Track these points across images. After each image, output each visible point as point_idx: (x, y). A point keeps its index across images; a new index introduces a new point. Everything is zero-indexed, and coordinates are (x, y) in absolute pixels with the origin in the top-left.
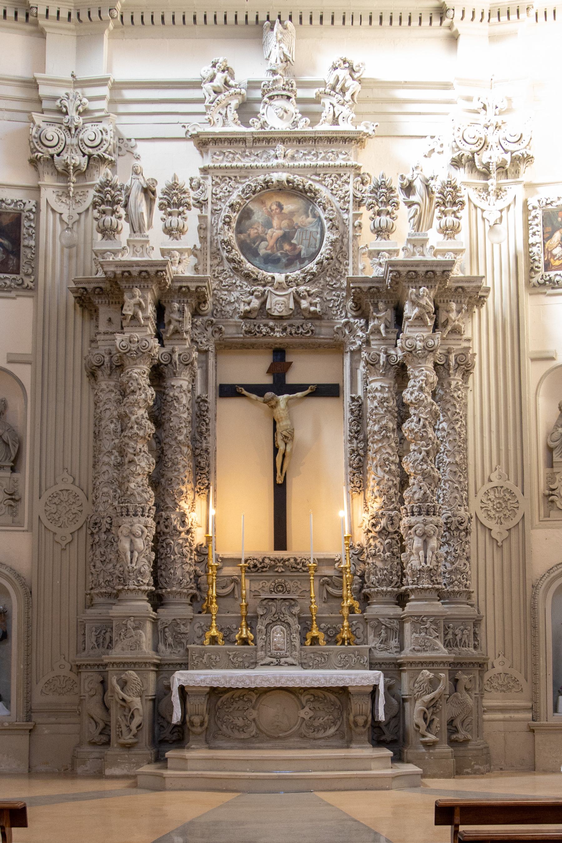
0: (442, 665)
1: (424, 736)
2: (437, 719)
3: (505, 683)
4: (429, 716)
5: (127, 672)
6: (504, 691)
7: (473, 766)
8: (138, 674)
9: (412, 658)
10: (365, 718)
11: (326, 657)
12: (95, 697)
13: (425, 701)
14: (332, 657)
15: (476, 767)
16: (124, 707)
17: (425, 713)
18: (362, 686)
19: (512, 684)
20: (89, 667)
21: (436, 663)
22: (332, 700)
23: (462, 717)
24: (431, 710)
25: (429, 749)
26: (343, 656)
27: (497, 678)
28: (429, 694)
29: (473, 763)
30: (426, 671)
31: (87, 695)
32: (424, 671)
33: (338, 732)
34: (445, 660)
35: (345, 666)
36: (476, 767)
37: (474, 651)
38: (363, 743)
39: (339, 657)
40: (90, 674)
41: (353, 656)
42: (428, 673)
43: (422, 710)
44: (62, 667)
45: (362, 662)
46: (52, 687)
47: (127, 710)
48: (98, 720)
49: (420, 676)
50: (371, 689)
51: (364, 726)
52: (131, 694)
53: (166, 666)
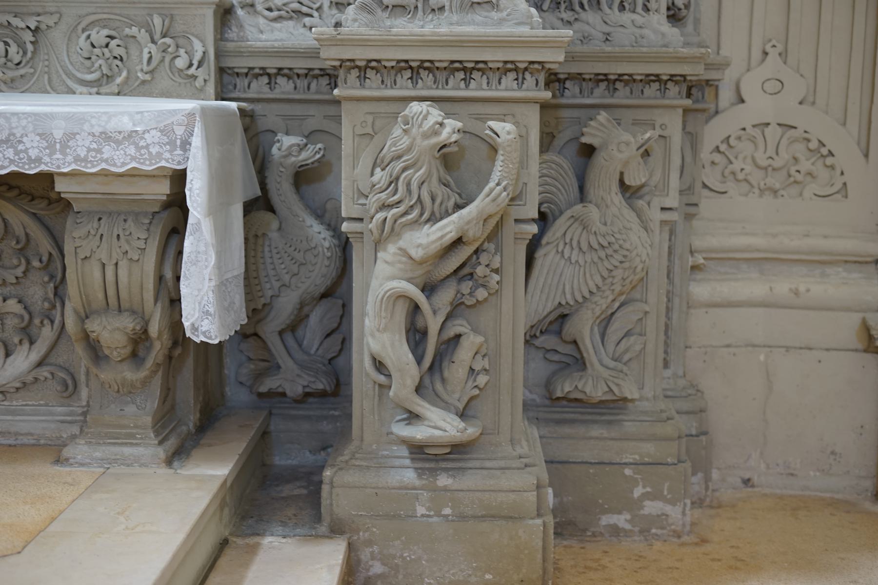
0: (509, 80)
1: (413, 417)
2: (471, 342)
3: (778, 163)
4: (433, 324)
6: (775, 192)
7: (638, 504)
9: (363, 43)
10: (128, 323)
11: (28, 37)
13: (417, 254)
14: (57, 36)
15: (652, 507)
17: (416, 308)
18: (105, 174)
19: (805, 165)
21: (481, 67)
22: (19, 231)
23: (601, 304)
24: (445, 297)
25: (433, 472)
26: (99, 36)
27: (753, 140)
28: (433, 219)
29: (638, 492)
30: (424, 106)
32: (416, 107)
33: (44, 372)
34: (523, 56)
35: (109, 78)
36: (652, 507)
37: (666, 28)
38: (129, 439)
39: (82, 41)
41: (143, 36)
42: (435, 114)
43: (402, 296)
45: (181, 63)
49: (397, 132)
50: (163, 189)
51: (135, 356)
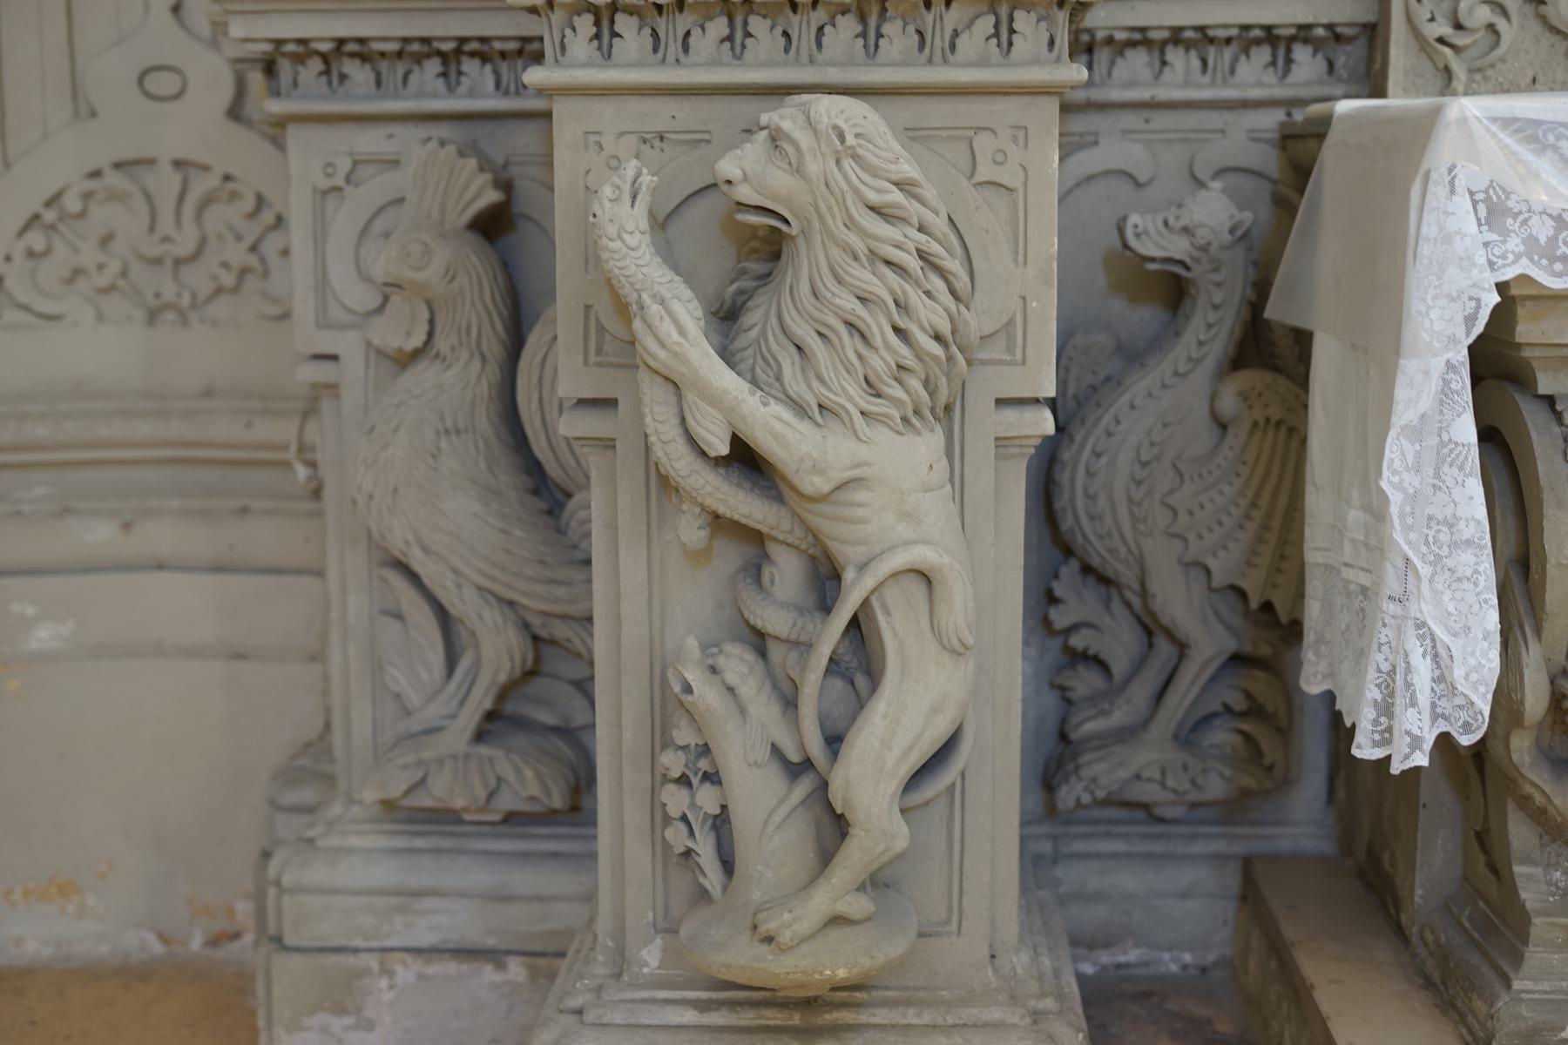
5: (785, 117)
8: (913, 135)
12: (424, 374)
16: (755, 538)
20: (360, 75)
31: (348, 345)
40: (371, 141)
44: (163, 84)
46: (89, 255)
47: (787, 573)
48: (463, 603)
52: (849, 394)
53: (1138, 60)
